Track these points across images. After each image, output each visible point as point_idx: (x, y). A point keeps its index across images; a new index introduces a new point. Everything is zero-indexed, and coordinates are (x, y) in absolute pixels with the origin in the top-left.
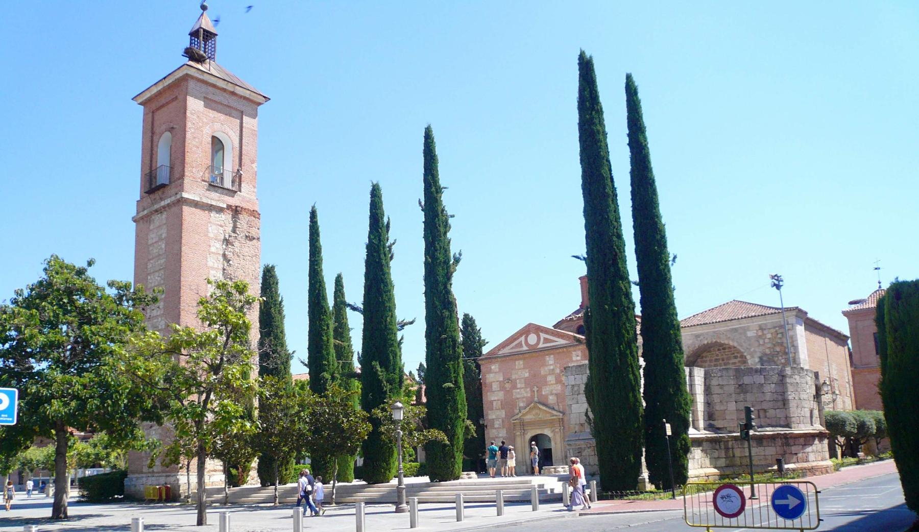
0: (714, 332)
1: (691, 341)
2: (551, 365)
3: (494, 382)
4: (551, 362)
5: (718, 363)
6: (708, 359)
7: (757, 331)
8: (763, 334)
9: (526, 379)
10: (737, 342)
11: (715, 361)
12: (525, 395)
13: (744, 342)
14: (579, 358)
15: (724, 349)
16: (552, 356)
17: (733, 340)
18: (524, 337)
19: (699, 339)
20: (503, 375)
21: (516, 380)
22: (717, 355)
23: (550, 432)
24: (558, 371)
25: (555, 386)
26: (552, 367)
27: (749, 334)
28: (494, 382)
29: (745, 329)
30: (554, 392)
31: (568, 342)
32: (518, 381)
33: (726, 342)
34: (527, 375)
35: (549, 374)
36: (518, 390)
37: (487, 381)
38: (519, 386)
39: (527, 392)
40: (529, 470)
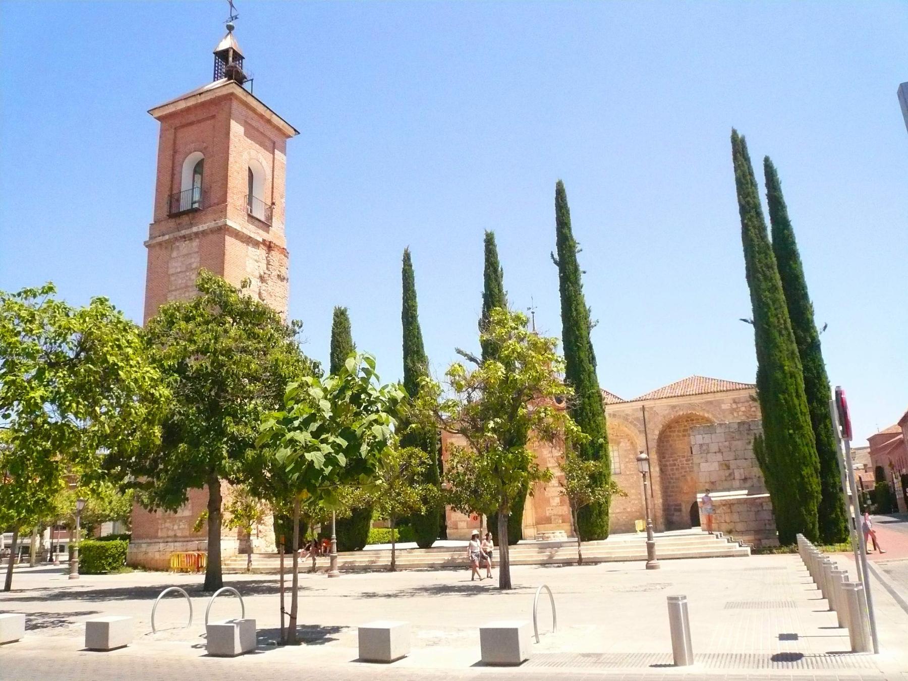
0: (690, 404)
1: (667, 412)
5: (686, 433)
6: (677, 429)
7: (731, 404)
8: (737, 408)
10: (712, 414)
11: (683, 432)
13: (719, 414)
15: (692, 420)
17: (708, 412)
19: (675, 410)
22: (685, 426)
27: (724, 407)
29: (719, 403)
33: (701, 414)
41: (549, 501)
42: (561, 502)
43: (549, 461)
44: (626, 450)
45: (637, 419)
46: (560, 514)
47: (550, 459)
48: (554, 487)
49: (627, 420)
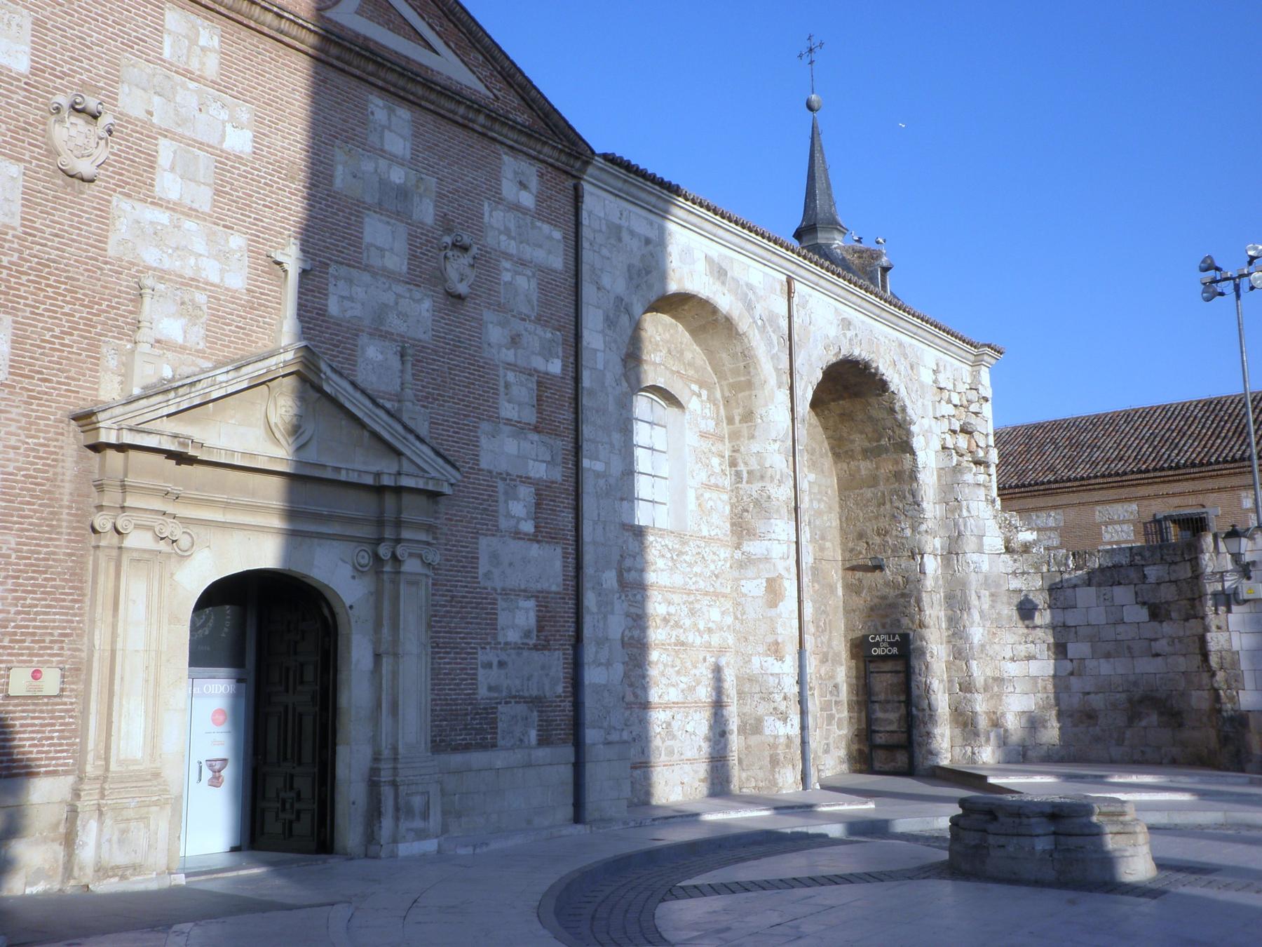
2: (393, 159)
4: (397, 144)
9: (225, 161)
12: (211, 270)
14: (527, 199)
19: (849, 334)
20: (38, 46)
21: (150, 132)
23: (347, 570)
24: (426, 212)
25: (400, 289)
26: (397, 176)
31: (481, 87)
32: (166, 151)
34: (239, 141)
35: (379, 208)
36: (163, 217)
38: (169, 185)
39: (223, 256)
40: (304, 826)
41: (493, 625)
42: (540, 629)
43: (507, 385)
44: (704, 435)
45: (772, 319)
46: (535, 693)
47: (511, 377)
48: (517, 535)
49: (750, 307)
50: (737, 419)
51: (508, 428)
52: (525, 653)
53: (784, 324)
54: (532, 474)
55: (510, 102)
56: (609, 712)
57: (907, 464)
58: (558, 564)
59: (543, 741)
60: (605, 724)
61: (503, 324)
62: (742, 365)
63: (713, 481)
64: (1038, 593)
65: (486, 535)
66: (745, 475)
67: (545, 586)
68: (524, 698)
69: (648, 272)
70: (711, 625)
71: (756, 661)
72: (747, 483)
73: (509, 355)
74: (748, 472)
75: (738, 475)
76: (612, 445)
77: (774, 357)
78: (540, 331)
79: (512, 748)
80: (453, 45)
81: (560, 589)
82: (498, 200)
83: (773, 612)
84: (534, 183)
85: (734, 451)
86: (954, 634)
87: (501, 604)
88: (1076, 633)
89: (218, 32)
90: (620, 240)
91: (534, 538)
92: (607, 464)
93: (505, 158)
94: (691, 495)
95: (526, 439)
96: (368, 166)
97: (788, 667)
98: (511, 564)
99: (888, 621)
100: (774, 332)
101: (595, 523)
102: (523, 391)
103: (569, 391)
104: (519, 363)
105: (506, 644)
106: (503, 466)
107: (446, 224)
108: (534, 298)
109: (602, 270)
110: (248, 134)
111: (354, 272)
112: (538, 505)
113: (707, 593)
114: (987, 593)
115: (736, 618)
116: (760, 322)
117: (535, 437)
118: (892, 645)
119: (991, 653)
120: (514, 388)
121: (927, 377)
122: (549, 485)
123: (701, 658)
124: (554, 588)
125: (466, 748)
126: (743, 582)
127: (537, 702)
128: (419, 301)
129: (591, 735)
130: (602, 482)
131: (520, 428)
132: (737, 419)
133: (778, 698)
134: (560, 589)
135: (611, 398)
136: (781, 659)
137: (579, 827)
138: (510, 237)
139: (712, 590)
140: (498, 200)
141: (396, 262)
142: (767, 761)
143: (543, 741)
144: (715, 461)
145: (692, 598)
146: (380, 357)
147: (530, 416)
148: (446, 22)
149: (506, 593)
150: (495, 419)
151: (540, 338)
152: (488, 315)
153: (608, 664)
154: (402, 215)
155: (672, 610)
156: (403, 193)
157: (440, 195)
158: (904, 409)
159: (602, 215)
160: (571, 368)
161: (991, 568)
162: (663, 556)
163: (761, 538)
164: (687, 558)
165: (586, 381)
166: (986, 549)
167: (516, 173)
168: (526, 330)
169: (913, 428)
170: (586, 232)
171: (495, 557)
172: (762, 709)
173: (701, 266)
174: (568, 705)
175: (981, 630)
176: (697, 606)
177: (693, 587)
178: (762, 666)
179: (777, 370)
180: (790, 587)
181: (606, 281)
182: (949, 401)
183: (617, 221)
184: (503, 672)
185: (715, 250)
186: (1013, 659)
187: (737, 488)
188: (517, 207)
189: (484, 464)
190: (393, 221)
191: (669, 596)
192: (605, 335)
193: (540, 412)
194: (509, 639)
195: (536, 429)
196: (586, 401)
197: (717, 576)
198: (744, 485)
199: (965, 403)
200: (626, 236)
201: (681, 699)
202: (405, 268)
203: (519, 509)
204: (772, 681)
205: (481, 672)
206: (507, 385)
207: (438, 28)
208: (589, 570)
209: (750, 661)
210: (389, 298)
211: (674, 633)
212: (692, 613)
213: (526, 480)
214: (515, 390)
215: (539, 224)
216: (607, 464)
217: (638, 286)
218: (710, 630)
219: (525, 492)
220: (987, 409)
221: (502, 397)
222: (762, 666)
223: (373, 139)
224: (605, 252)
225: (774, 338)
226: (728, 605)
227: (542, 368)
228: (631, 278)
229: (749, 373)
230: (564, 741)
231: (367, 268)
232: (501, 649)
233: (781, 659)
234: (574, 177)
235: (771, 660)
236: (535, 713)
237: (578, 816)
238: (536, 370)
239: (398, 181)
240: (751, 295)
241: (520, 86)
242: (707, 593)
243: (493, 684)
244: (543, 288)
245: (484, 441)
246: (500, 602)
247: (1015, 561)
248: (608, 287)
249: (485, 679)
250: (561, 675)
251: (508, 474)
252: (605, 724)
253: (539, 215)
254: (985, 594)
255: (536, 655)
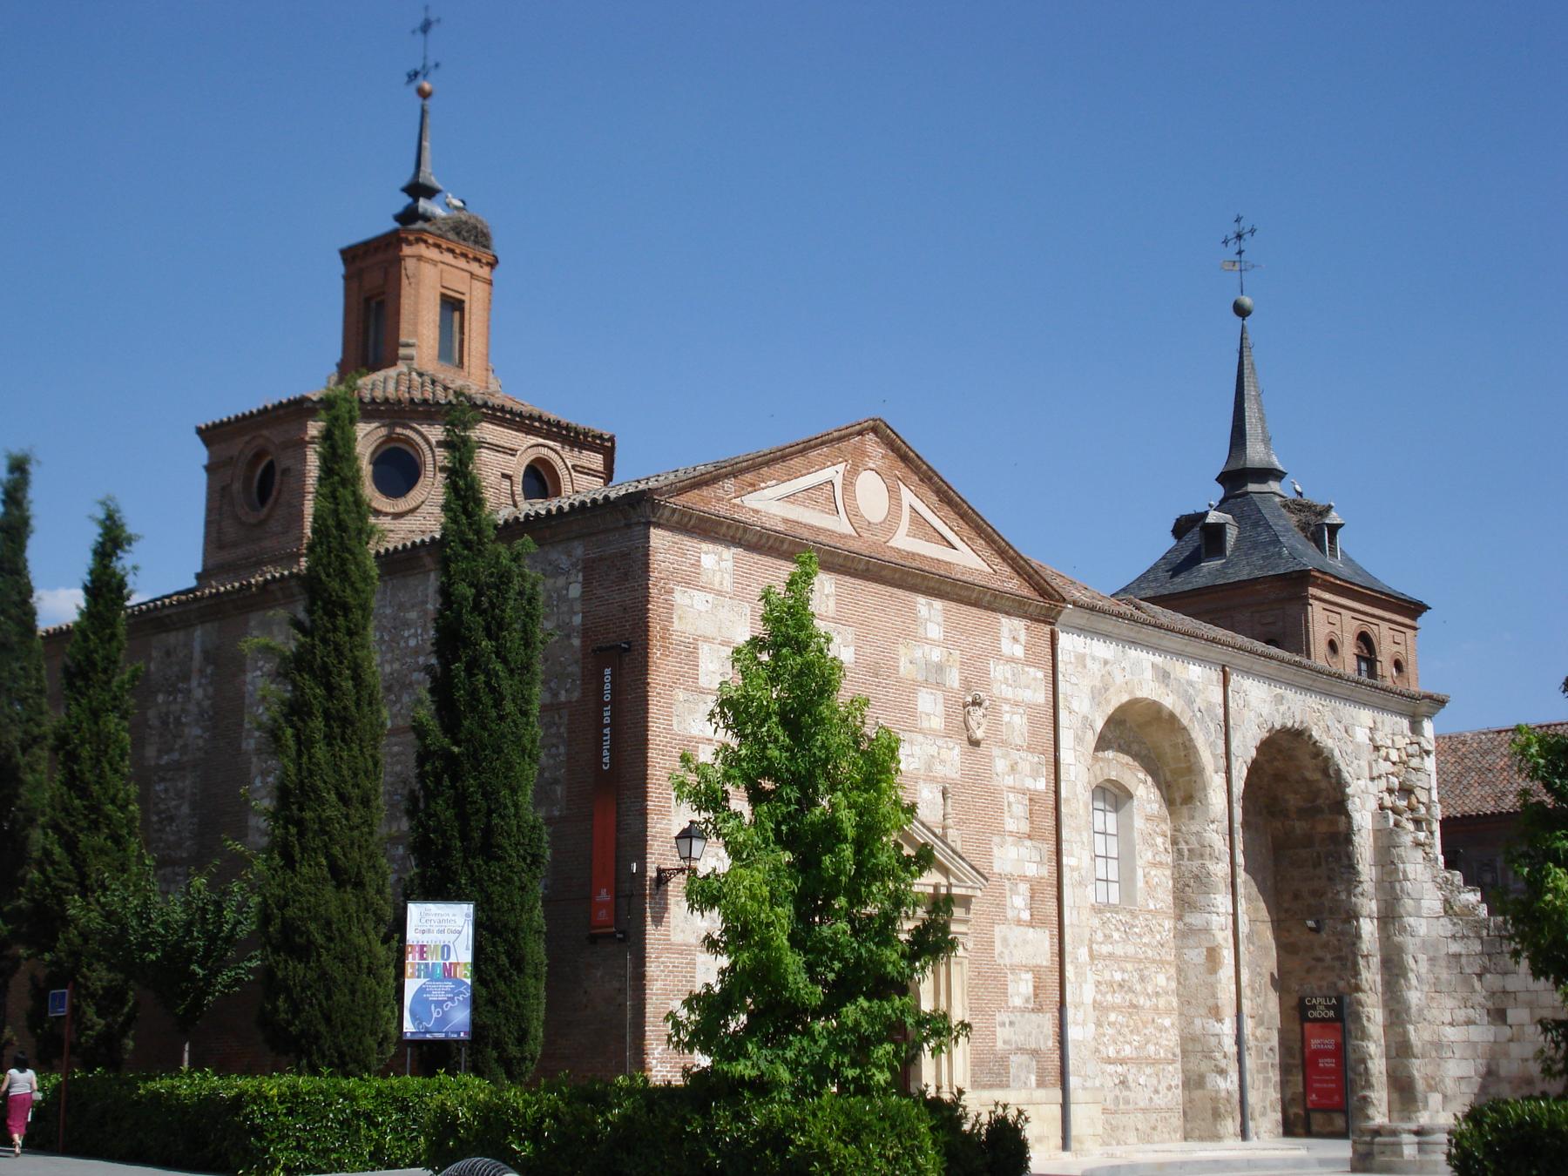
2: (933, 643)
3: (706, 639)
4: (935, 631)
14: (1019, 651)
16: (938, 604)
18: (841, 467)
19: (1282, 709)
24: (954, 679)
25: (940, 742)
26: (936, 655)
28: (706, 639)
30: (940, 770)
37: (677, 625)
41: (1005, 994)
42: (1036, 995)
45: (1210, 707)
46: (1033, 1046)
47: (1012, 797)
48: (1019, 922)
49: (1190, 702)
50: (1178, 801)
51: (1012, 838)
52: (1027, 1015)
53: (1221, 711)
54: (1027, 874)
55: (1013, 584)
56: (1085, 1063)
57: (1342, 826)
58: (1047, 944)
59: (1041, 1084)
60: (1083, 1073)
61: (1004, 757)
62: (1182, 754)
63: (1158, 859)
64: (1477, 957)
65: (998, 924)
66: (1186, 853)
67: (1039, 962)
68: (1027, 1050)
69: (1106, 690)
70: (1158, 989)
71: (1198, 1022)
72: (1188, 860)
73: (1009, 780)
74: (1189, 850)
75: (1180, 852)
76: (1083, 843)
77: (1212, 745)
78: (1030, 757)
79: (1020, 1089)
80: (965, 539)
81: (1049, 964)
82: (999, 656)
83: (1211, 979)
84: (1023, 636)
85: (1175, 830)
86: (1392, 998)
87: (1010, 977)
88: (1515, 999)
89: (833, 581)
90: (1085, 667)
91: (1031, 925)
92: (1080, 859)
93: (1003, 620)
94: (1140, 873)
95: (1023, 845)
96: (918, 653)
97: (1227, 1028)
98: (1015, 946)
99: (1324, 984)
100: (1211, 721)
101: (1072, 908)
102: (1020, 808)
103: (1052, 803)
104: (1018, 785)
105: (1014, 1007)
106: (1008, 869)
107: (967, 685)
108: (1025, 731)
109: (1072, 696)
110: (852, 649)
111: (914, 735)
112: (1032, 897)
113: (1154, 961)
114: (1425, 957)
115: (1179, 983)
116: (1199, 714)
117: (1028, 843)
118: (1328, 1007)
119: (1429, 1017)
120: (1014, 806)
121: (1362, 735)
122: (1039, 881)
123: (1150, 1019)
124: (1045, 963)
125: (991, 1086)
126: (1186, 951)
127: (1035, 1053)
128: (953, 748)
129: (1074, 1081)
130: (1075, 874)
131: (1020, 837)
132: (1178, 801)
133: (1218, 1056)
134: (1049, 964)
135: (1081, 804)
136: (1220, 1020)
137: (1067, 1154)
138: (1009, 685)
139: (1158, 958)
140: (999, 656)
141: (937, 723)
142: (1209, 1115)
143: (1041, 1084)
144: (1159, 840)
145: (1142, 966)
146: (931, 796)
147: (1025, 827)
148: (961, 522)
149: (1013, 968)
150: (1002, 833)
151: (1031, 763)
152: (996, 751)
153: (1084, 1024)
154: (939, 685)
155: (1126, 976)
156: (940, 668)
157: (962, 663)
158: (1338, 771)
159: (1071, 648)
160: (1052, 784)
161: (1428, 931)
162: (1118, 930)
163: (1201, 910)
164: (1137, 930)
165: (1063, 794)
166: (1424, 912)
167: (1010, 631)
168: (1021, 758)
169: (1348, 790)
170: (1061, 667)
171: (1005, 941)
172: (1204, 1066)
173: (1149, 674)
174: (1056, 1056)
175: (1418, 994)
176: (1146, 973)
177: (1142, 956)
178: (1203, 1028)
179: (1214, 756)
180: (1227, 955)
181: (1075, 706)
182: (1387, 759)
183: (1082, 651)
184: (1012, 1029)
185: (1158, 659)
186: (1451, 1024)
187: (1179, 864)
188: (1012, 660)
189: (996, 870)
190: (934, 691)
191: (1123, 965)
192: (1075, 750)
193: (1032, 822)
194: (1016, 1004)
195: (1030, 837)
196: (1064, 809)
197: (1162, 946)
198: (1185, 862)
199: (1404, 758)
200: (1089, 662)
201: (1134, 1055)
202: (943, 726)
203: (1018, 902)
204: (1213, 1041)
205: (998, 1029)
206: (1009, 805)
207: (956, 529)
208: (1068, 948)
209: (1193, 1022)
210: (933, 750)
211: (1127, 997)
212: (1142, 979)
213: (1024, 878)
214: (1014, 808)
215: (1027, 669)
216: (1080, 859)
217: (1099, 704)
218: (1157, 994)
219: (1024, 888)
220: (1430, 764)
221: (1007, 814)
222: (1203, 1028)
223: (921, 630)
224: (1074, 680)
225: (1212, 726)
226: (1173, 971)
227: (1032, 787)
228: (1093, 698)
229: (1189, 761)
230: (1054, 1085)
231: (921, 731)
232: (1011, 1012)
233: (1220, 1020)
234: (1050, 624)
235: (1212, 1021)
236: (1034, 1063)
237: (1065, 1146)
238: (1028, 790)
239: (936, 660)
240: (1191, 691)
241: (1012, 559)
242: (1154, 961)
243: (1007, 1038)
244: (1032, 721)
245: (995, 850)
246: (1009, 975)
247: (1454, 924)
248: (1077, 710)
249: (1002, 1034)
250: (1051, 1033)
251: (1012, 875)
252: (1083, 1073)
253: (1028, 662)
254: (1422, 957)
255: (1033, 1016)
